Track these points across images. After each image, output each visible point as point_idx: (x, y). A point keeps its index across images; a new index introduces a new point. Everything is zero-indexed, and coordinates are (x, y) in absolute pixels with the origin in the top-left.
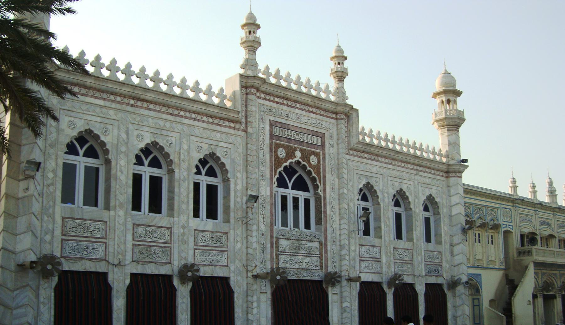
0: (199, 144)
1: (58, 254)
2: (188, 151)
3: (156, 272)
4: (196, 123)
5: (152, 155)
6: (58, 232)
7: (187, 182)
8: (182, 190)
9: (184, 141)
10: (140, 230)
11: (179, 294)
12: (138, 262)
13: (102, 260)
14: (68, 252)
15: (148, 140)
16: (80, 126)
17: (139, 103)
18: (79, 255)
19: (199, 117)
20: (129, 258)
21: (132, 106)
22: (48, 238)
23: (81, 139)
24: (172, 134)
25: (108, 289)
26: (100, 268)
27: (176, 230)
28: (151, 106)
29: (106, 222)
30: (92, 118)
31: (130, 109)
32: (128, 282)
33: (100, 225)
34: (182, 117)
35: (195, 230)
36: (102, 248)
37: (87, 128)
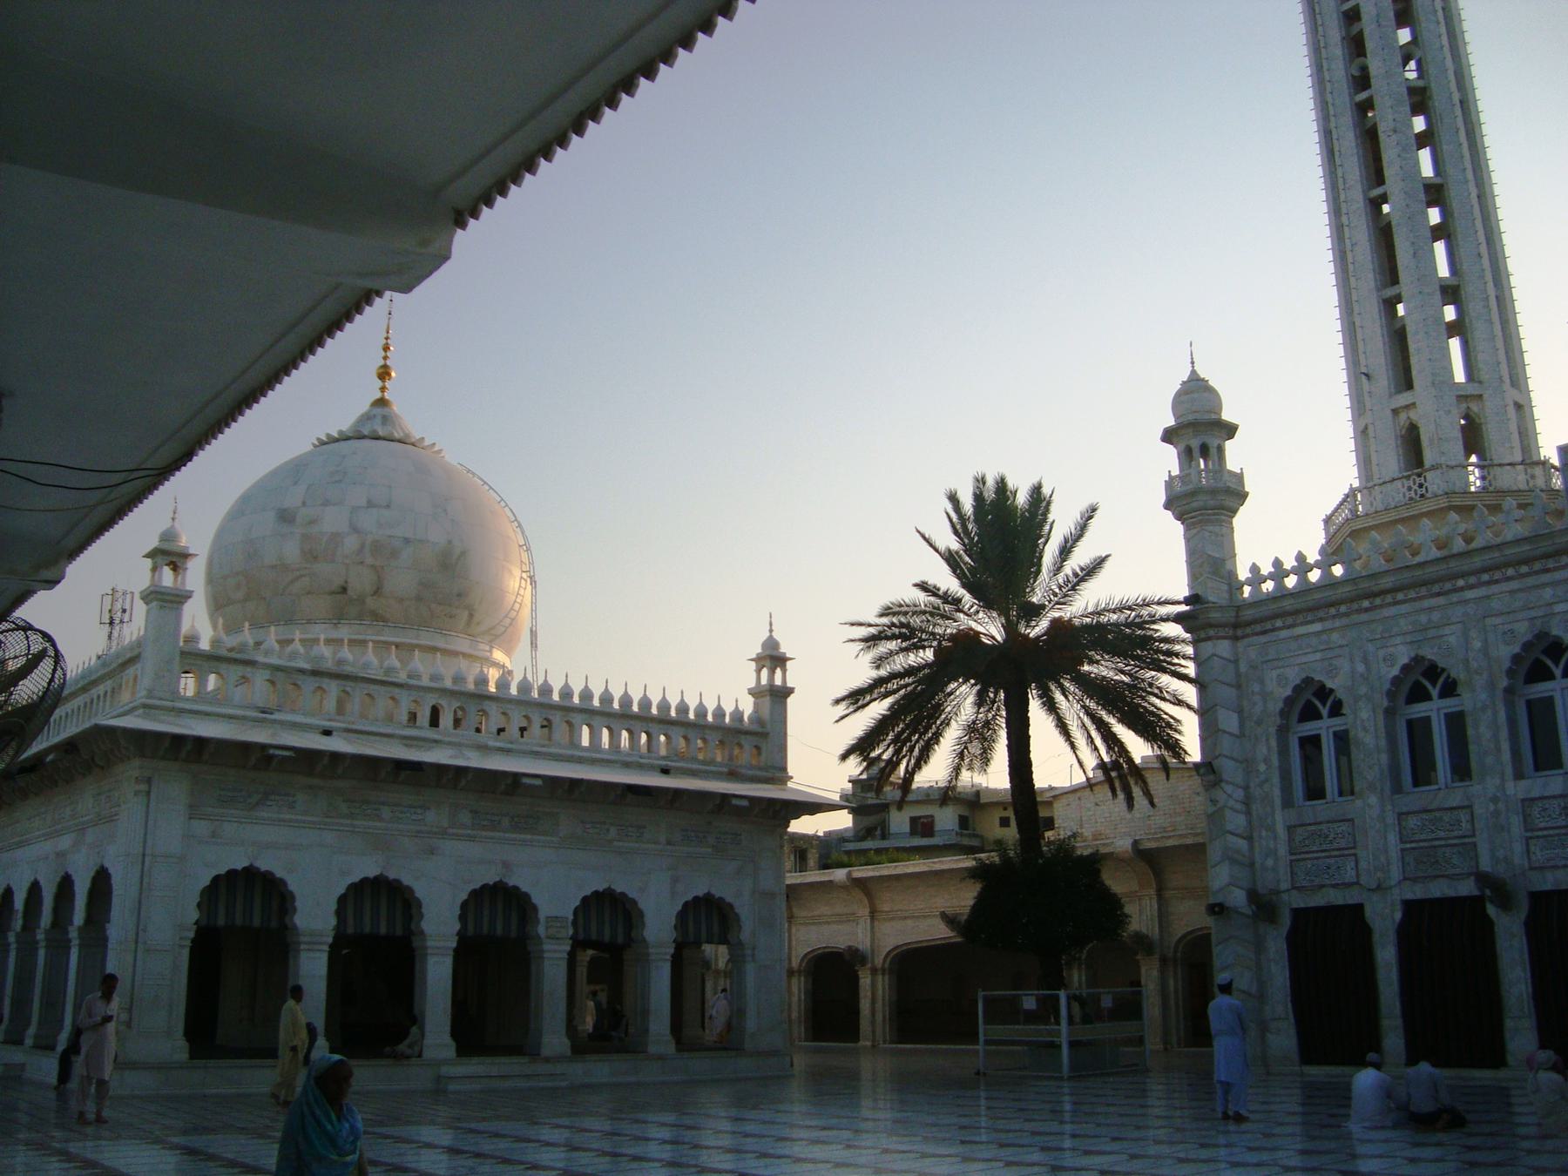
0: (1507, 627)
1: (1284, 886)
2: (1485, 651)
3: (1451, 893)
4: (1495, 588)
5: (1423, 679)
6: (1283, 850)
7: (1489, 712)
8: (1482, 729)
9: (1473, 634)
10: (1412, 822)
11: (1499, 930)
12: (1415, 880)
13: (1350, 885)
16: (1294, 676)
17: (1378, 601)
18: (1317, 881)
19: (1497, 575)
20: (1395, 874)
21: (1367, 610)
22: (1270, 862)
24: (1447, 631)
27: (1478, 810)
28: (1400, 596)
29: (1352, 820)
30: (1311, 658)
31: (1364, 617)
32: (1398, 916)
33: (1344, 827)
34: (1462, 589)
35: (1523, 800)
36: (1350, 864)
37: (1304, 676)
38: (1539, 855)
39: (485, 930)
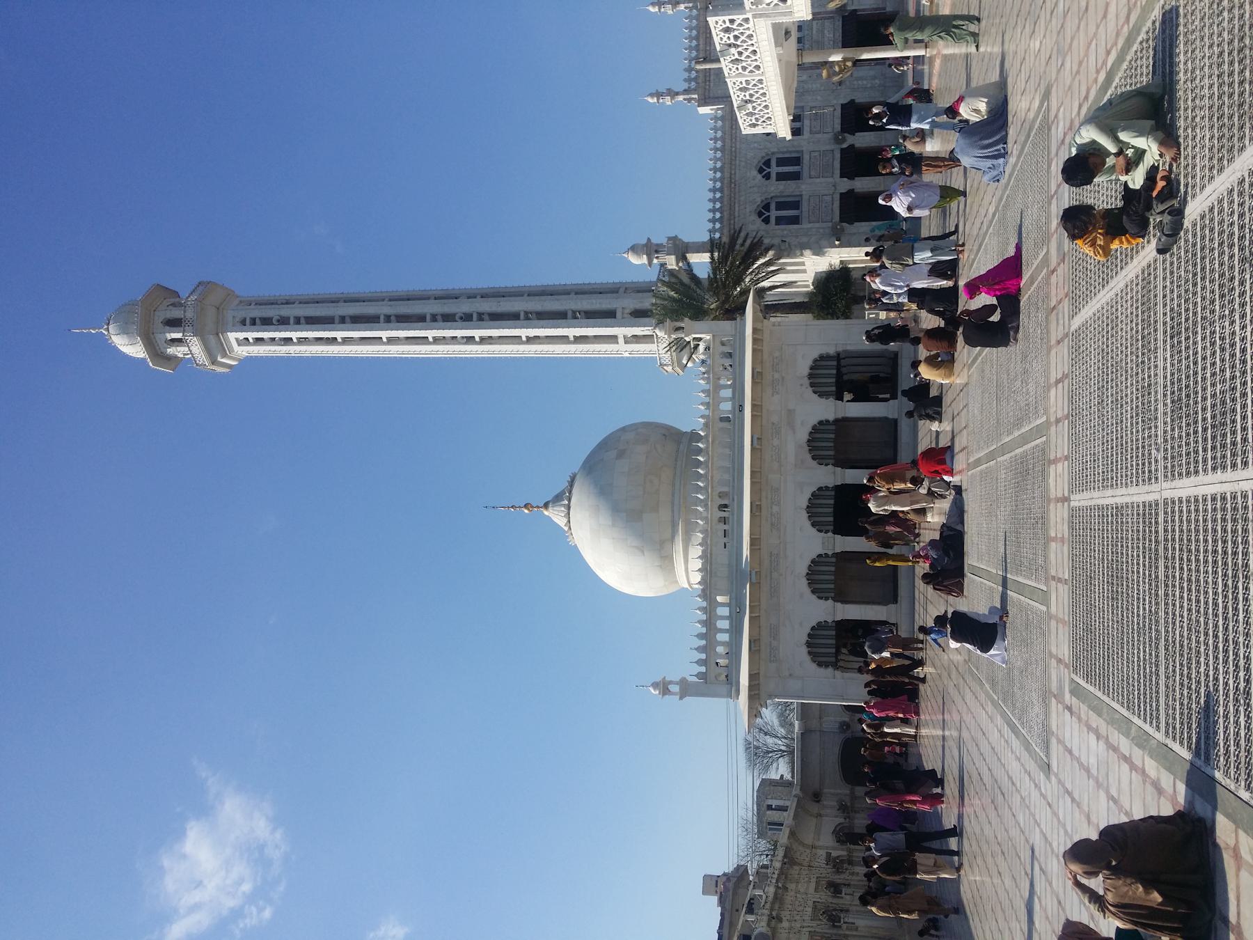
6: (817, 225)
10: (813, 173)
14: (829, 218)
15: (755, 173)
16: (754, 217)
20: (830, 180)
23: (760, 214)
25: (851, 192)
26: (837, 197)
38: (830, 130)
39: (833, 569)
